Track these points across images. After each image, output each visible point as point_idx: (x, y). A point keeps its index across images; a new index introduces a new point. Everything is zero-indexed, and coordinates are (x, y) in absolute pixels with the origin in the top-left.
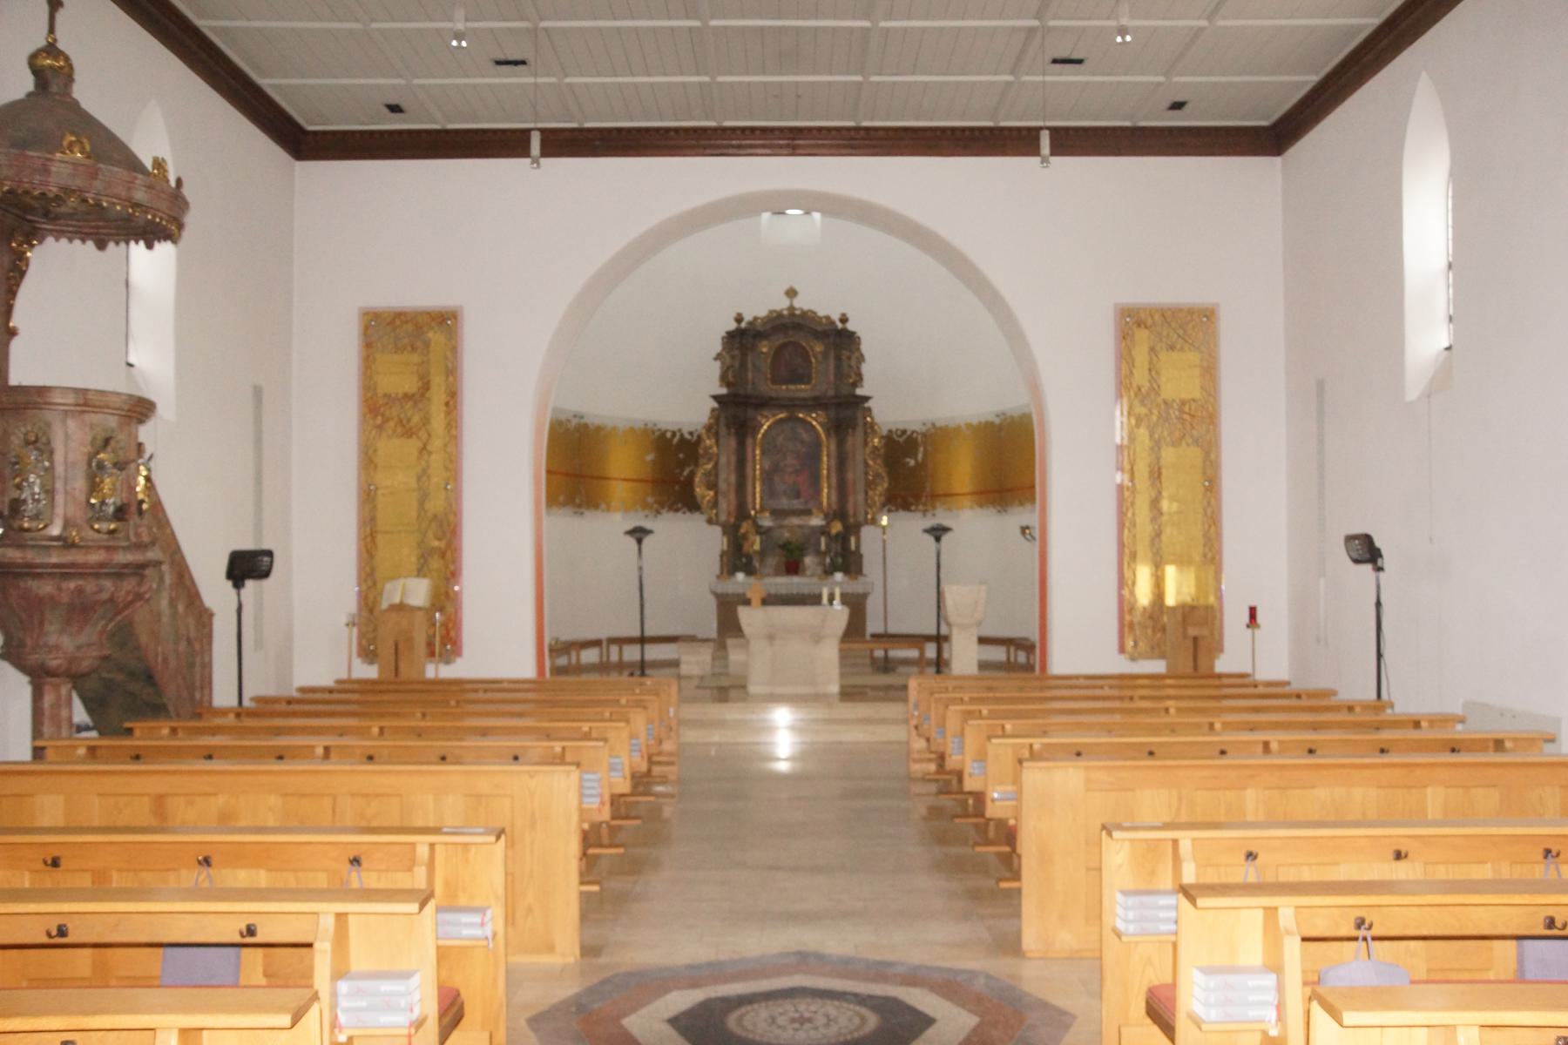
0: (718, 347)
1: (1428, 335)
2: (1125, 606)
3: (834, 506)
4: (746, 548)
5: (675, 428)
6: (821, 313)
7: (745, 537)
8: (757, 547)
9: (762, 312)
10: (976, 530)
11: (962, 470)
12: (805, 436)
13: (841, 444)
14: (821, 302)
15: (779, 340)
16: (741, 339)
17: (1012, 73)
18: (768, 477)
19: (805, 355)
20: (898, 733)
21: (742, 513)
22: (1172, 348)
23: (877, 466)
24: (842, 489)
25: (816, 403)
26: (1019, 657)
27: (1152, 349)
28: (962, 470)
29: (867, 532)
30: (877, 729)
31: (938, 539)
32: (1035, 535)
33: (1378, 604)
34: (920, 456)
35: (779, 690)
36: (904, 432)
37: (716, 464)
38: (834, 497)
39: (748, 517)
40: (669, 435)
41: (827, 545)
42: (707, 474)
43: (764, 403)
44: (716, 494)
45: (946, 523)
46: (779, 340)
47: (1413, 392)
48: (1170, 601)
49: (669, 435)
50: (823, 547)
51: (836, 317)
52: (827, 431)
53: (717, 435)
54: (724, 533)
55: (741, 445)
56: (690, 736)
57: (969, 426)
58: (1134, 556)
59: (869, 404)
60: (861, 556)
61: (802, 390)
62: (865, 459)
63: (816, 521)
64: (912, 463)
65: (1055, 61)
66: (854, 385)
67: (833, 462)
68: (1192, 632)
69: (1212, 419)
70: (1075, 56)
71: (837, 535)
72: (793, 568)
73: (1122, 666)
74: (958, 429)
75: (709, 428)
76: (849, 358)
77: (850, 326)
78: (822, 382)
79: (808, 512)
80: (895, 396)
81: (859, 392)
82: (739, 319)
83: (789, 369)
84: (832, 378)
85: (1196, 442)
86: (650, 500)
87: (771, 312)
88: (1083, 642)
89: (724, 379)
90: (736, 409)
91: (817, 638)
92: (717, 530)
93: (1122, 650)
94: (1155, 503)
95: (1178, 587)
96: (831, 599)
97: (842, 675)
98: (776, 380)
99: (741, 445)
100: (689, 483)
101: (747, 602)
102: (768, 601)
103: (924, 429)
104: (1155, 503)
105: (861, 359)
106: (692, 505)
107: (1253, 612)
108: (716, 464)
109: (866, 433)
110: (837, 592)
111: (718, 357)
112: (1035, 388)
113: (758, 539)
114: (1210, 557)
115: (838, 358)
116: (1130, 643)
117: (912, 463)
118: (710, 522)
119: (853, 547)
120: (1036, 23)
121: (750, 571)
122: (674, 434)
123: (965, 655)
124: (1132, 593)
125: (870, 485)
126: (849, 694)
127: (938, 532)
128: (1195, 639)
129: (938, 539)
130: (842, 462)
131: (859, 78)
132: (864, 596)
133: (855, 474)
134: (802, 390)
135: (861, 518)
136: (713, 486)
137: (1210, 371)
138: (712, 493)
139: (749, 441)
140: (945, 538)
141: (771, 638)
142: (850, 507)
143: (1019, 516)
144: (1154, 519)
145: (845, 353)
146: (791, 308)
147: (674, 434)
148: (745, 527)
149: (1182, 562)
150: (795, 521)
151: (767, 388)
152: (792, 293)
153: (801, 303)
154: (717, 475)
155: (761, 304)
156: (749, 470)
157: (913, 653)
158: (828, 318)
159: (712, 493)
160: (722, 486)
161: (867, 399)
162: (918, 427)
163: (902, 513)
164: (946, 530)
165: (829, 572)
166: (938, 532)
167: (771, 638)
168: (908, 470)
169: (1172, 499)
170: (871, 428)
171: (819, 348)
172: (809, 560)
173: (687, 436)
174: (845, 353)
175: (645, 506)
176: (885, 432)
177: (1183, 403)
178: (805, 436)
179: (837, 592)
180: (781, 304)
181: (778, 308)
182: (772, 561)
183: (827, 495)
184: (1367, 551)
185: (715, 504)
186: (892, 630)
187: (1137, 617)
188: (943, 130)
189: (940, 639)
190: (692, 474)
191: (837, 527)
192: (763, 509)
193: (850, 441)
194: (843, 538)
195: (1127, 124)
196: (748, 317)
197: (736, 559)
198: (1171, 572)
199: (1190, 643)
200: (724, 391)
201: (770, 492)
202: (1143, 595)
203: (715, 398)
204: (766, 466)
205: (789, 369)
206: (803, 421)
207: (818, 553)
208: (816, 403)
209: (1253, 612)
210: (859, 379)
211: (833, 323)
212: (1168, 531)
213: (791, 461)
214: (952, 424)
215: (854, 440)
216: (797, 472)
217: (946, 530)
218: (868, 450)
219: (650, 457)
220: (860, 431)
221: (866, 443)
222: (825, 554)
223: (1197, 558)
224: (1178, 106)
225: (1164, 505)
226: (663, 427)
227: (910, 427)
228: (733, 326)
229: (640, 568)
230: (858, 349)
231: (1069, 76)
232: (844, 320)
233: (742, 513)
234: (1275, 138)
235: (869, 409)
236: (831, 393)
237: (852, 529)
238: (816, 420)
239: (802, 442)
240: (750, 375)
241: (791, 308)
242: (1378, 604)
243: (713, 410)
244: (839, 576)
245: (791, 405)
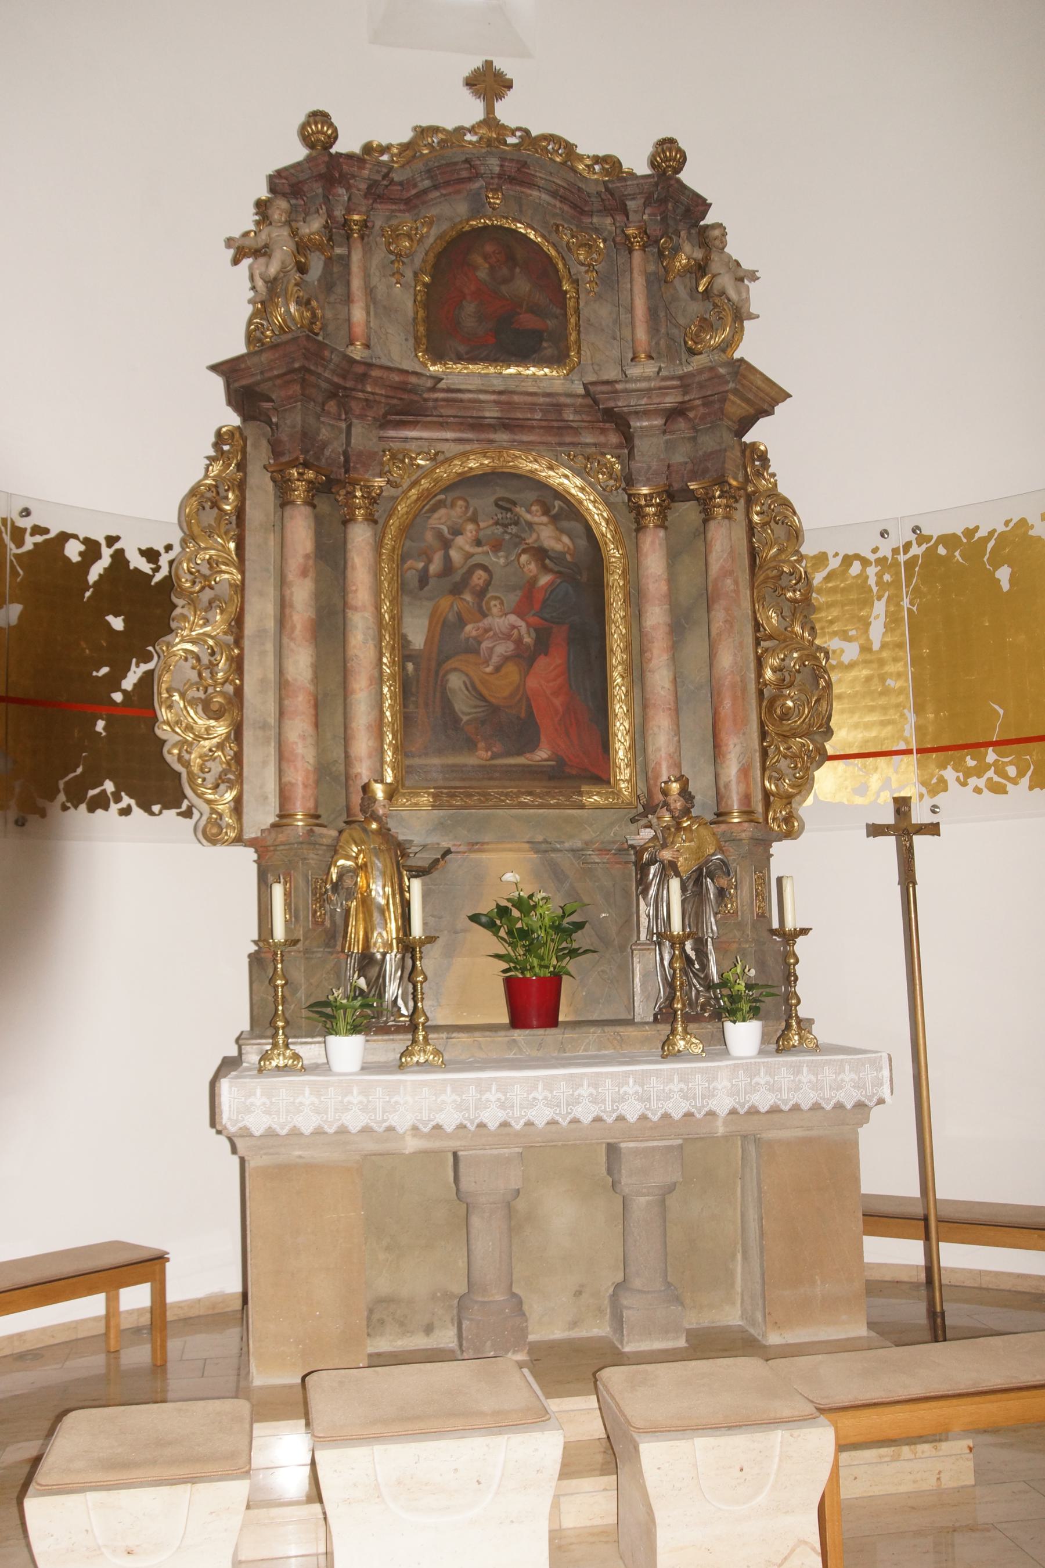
6: (588, 146)
12: (548, 537)
19: (544, 270)
37: (237, 624)
40: (73, 551)
43: (408, 405)
44: (237, 733)
46: (451, 213)
49: (73, 551)
55: (330, 555)
67: (656, 616)
76: (701, 269)
87: (423, 132)
98: (439, 336)
99: (330, 555)
103: (885, 551)
122: (92, 550)
138: (221, 729)
147: (92, 550)
152: (489, 83)
158: (610, 164)
159: (221, 729)
160: (259, 702)
173: (138, 562)
178: (548, 537)
182: (471, 979)
196: (347, 144)
204: (418, 639)
213: (503, 623)
214: (991, 523)
216: (525, 657)
228: (299, 153)
232: (669, 156)
239: (541, 554)
240: (358, 314)
241: (490, 121)
244: (744, 1035)
245: (513, 419)
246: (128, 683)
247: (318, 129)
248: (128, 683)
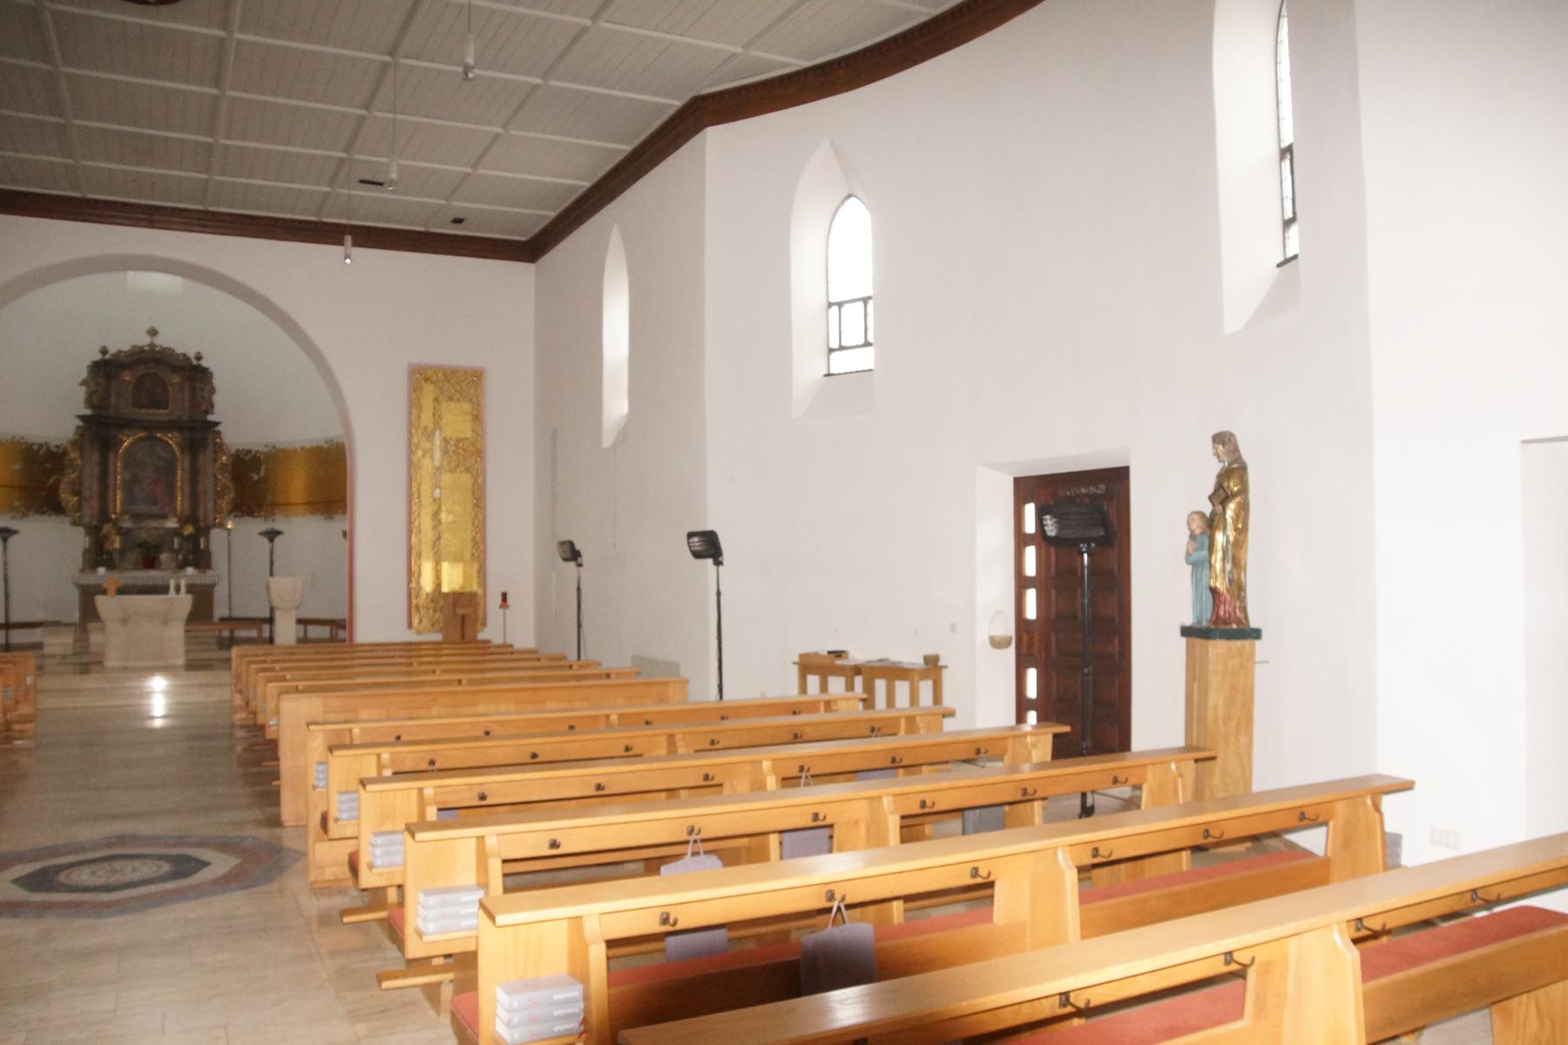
0: (84, 375)
1: (616, 405)
2: (412, 592)
3: (187, 512)
4: (107, 546)
5: (42, 441)
6: (179, 350)
7: (106, 537)
8: (117, 545)
9: (126, 347)
10: (303, 533)
11: (297, 484)
13: (194, 462)
14: (179, 339)
15: (141, 370)
16: (106, 370)
17: (331, 184)
18: (129, 487)
20: (224, 694)
21: (104, 516)
22: (451, 399)
23: (225, 480)
24: (194, 496)
25: (171, 426)
26: (331, 635)
27: (436, 399)
28: (297, 484)
29: (217, 536)
30: (214, 691)
31: (271, 540)
32: (348, 535)
33: (579, 590)
34: (262, 472)
35: (132, 664)
36: (249, 452)
37: (80, 476)
38: (187, 505)
39: (110, 520)
41: (181, 545)
42: (73, 483)
43: (125, 424)
44: (80, 501)
45: (277, 527)
46: (141, 370)
47: (607, 442)
48: (445, 589)
50: (176, 546)
51: (191, 355)
52: (182, 449)
53: (81, 449)
54: (88, 533)
56: (48, 702)
57: (303, 449)
58: (419, 555)
59: (219, 428)
60: (210, 554)
61: (161, 414)
62: (214, 475)
63: (172, 524)
64: (256, 477)
65: (362, 182)
66: (207, 412)
67: (187, 476)
68: (461, 611)
69: (479, 453)
70: (379, 180)
71: (189, 536)
72: (150, 563)
73: (411, 636)
74: (295, 450)
75: (74, 443)
77: (204, 363)
78: (177, 408)
79: (164, 517)
80: (246, 417)
81: (210, 418)
82: (104, 351)
83: (148, 397)
84: (187, 405)
85: (468, 470)
86: (17, 504)
88: (379, 619)
89: (89, 402)
90: (100, 427)
91: (165, 622)
92: (80, 531)
93: (410, 625)
94: (436, 515)
95: (453, 578)
96: (178, 589)
97: (188, 652)
98: (137, 404)
100: (54, 491)
101: (104, 592)
102: (123, 591)
104: (436, 515)
105: (213, 391)
106: (57, 508)
107: (504, 596)
108: (80, 476)
109: (215, 452)
110: (183, 583)
111: (84, 383)
112: (347, 424)
113: (118, 539)
114: (478, 555)
115: (193, 390)
116: (416, 621)
117: (256, 477)
118: (74, 523)
119: (202, 546)
120: (344, 155)
121: (111, 566)
122: (41, 446)
123: (286, 632)
124: (418, 583)
125: (219, 495)
126: (192, 666)
127: (272, 535)
128: (463, 617)
129: (271, 540)
130: (194, 474)
131: (204, 176)
132: (212, 587)
133: (206, 485)
134: (161, 414)
135: (210, 522)
136: (78, 493)
137: (477, 417)
139: (111, 456)
140: (278, 540)
141: (125, 621)
142: (201, 512)
143: (339, 524)
144: (435, 528)
145: (198, 385)
146: (152, 345)
148: (107, 528)
149: (455, 559)
150: (154, 524)
151: (130, 411)
152: (153, 332)
153: (162, 341)
154: (81, 484)
155: (124, 340)
156: (111, 481)
157: (253, 633)
160: (86, 493)
161: (217, 424)
162: (261, 449)
163: (247, 519)
164: (279, 533)
165: (182, 566)
166: (272, 535)
167: (125, 621)
168: (253, 484)
169: (449, 512)
170: (220, 448)
171: (176, 379)
172: (164, 557)
174: (198, 385)
175: (12, 509)
176: (233, 451)
177: (458, 441)
179: (183, 583)
180: (144, 341)
181: (140, 344)
182: (133, 556)
183: (181, 502)
184: (572, 554)
185: (79, 508)
186: (237, 613)
187: (422, 600)
188: (277, 220)
189: (270, 621)
190: (58, 483)
191: (189, 530)
192: (124, 513)
193: (201, 459)
194: (194, 539)
195: (422, 229)
196: (112, 350)
197: (98, 555)
198: (445, 565)
199: (459, 620)
200: (88, 412)
201: (130, 499)
202: (427, 584)
203: (82, 418)
205: (148, 397)
206: (160, 439)
207: (171, 550)
208: (171, 426)
209: (504, 596)
210: (210, 407)
211: (188, 359)
212: (446, 537)
214: (290, 447)
215: (205, 458)
217: (279, 533)
218: (218, 466)
219: (17, 467)
220: (210, 449)
221: (215, 461)
222: (178, 552)
223: (467, 556)
224: (458, 221)
225: (443, 516)
226: (31, 440)
227: (255, 448)
228: (98, 357)
229: (5, 564)
230: (210, 382)
231: (373, 193)
232: (199, 357)
233: (104, 516)
234: (531, 249)
235: (219, 433)
236: (185, 418)
237: (203, 531)
238: (172, 439)
240: (113, 399)
241: (152, 345)
242: (579, 590)
243: (78, 428)
244: (190, 570)
245: (151, 426)
246: (51, 481)
247: (104, 351)
248: (51, 481)
